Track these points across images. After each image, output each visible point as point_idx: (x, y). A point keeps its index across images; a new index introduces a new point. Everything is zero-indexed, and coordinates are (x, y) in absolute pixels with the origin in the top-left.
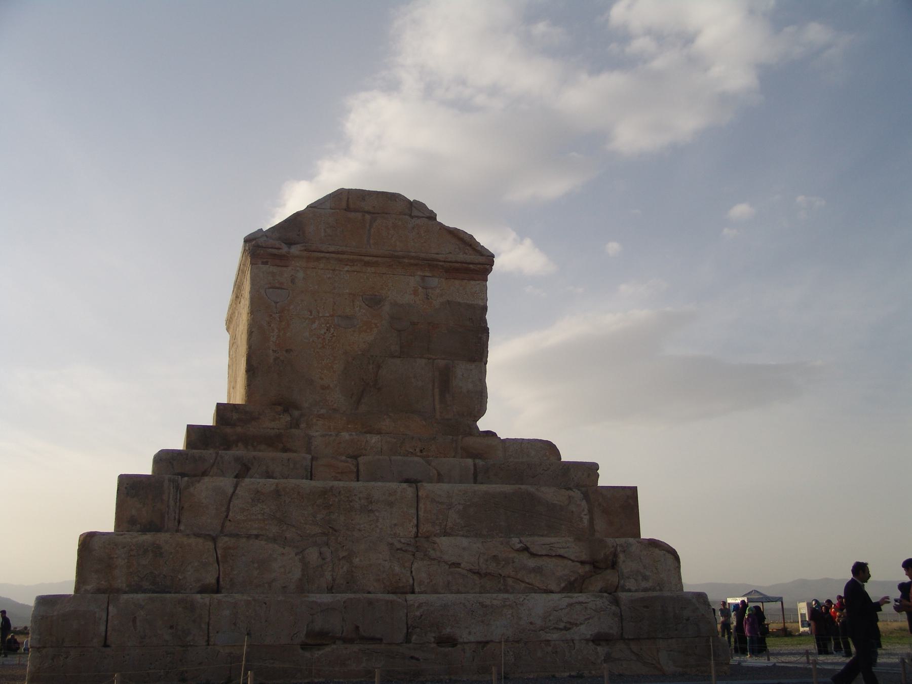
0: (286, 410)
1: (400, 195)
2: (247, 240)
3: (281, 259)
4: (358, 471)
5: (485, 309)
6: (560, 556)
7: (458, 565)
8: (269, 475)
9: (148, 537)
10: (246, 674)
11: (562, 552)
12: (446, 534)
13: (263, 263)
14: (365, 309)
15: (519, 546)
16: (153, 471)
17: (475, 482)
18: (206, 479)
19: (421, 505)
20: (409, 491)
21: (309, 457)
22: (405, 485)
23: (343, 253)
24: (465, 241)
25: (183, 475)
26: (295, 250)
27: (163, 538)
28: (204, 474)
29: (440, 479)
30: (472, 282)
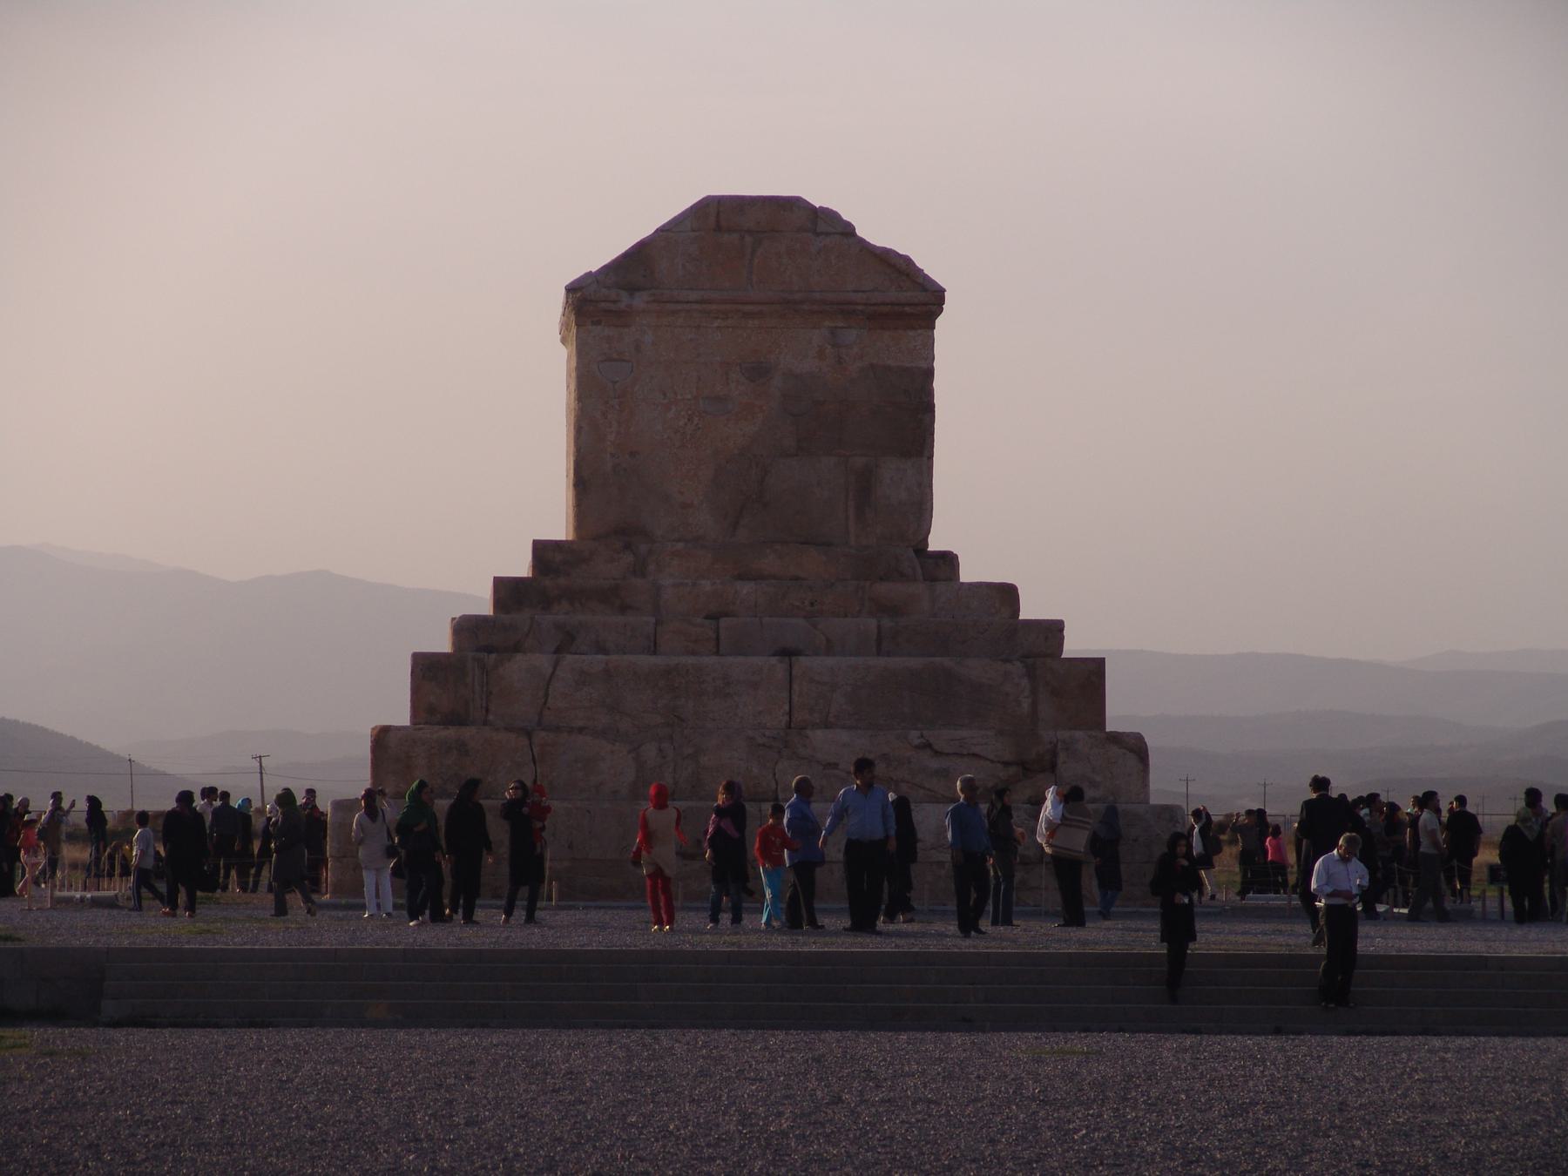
0: (627, 547)
1: (798, 199)
2: (571, 289)
3: (620, 317)
4: (718, 639)
5: (929, 374)
6: (975, 755)
7: (835, 766)
8: (602, 650)
9: (451, 732)
10: (550, 884)
11: (976, 750)
12: (827, 725)
13: (598, 323)
14: (760, 357)
15: (917, 742)
16: (454, 644)
17: (879, 653)
18: (519, 656)
19: (796, 687)
20: (777, 666)
21: (653, 620)
22: (774, 660)
23: (710, 302)
24: (897, 268)
25: (489, 650)
26: (640, 301)
27: (468, 732)
28: (517, 648)
29: (829, 650)
30: (911, 333)
